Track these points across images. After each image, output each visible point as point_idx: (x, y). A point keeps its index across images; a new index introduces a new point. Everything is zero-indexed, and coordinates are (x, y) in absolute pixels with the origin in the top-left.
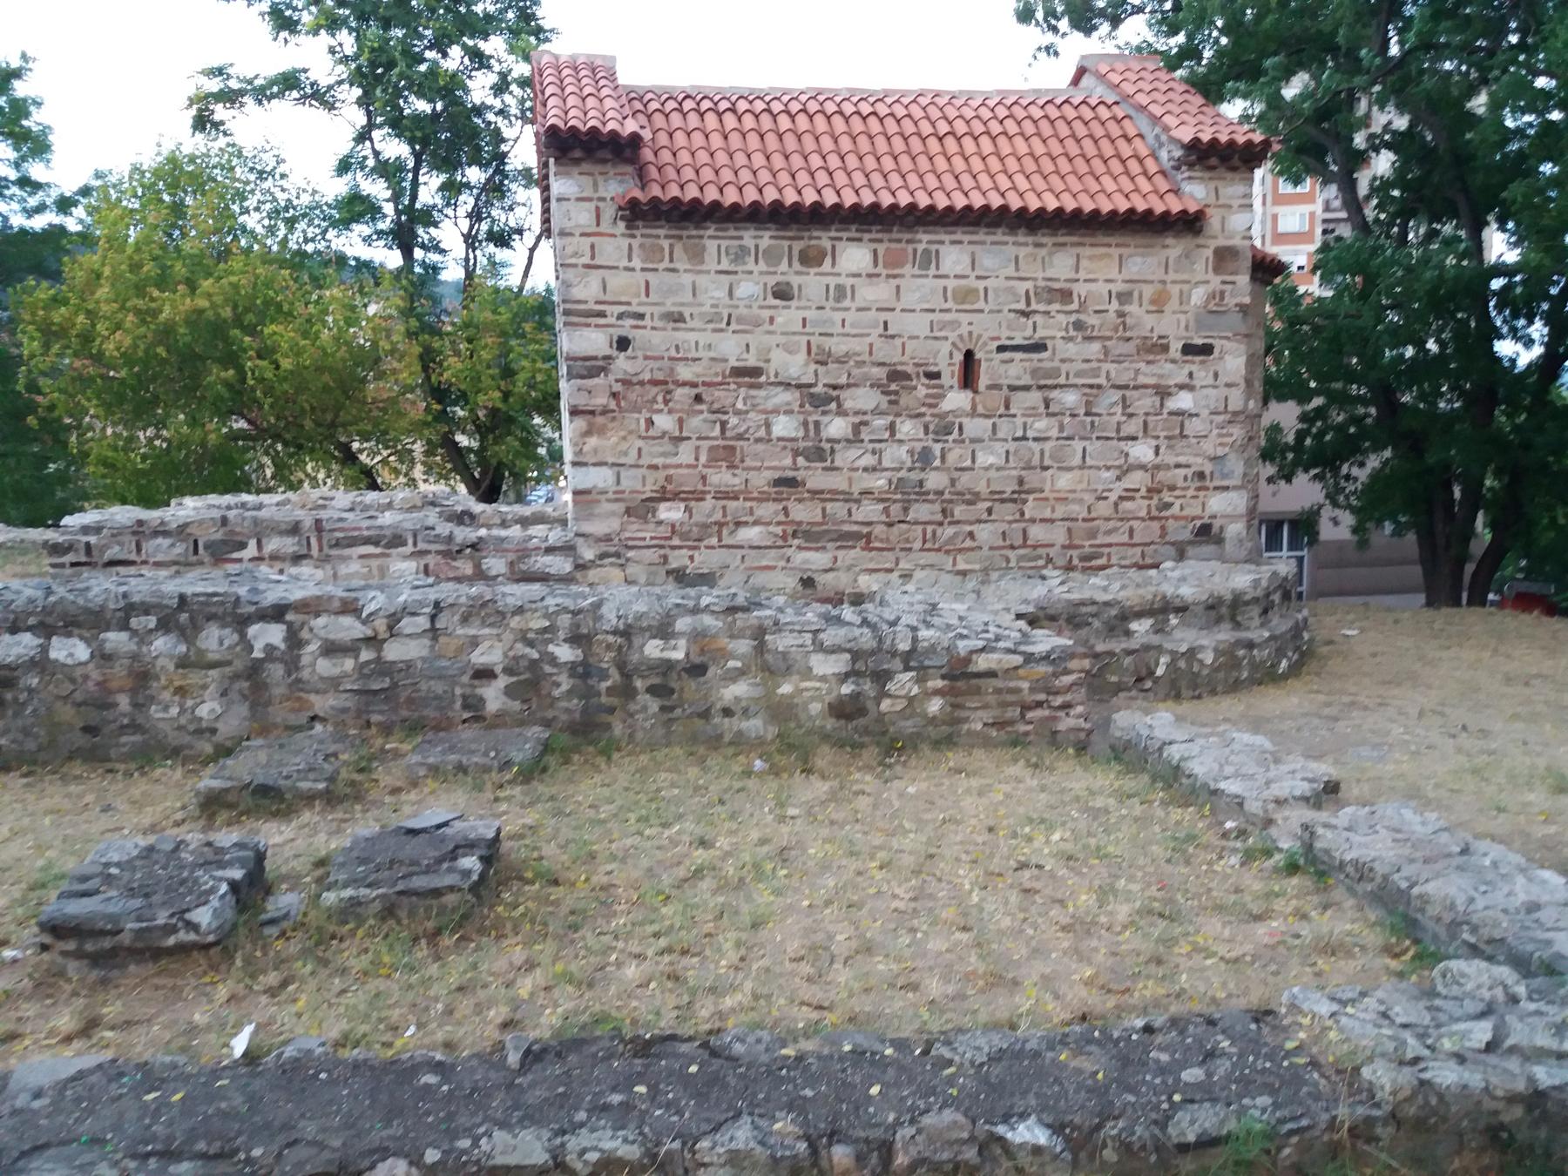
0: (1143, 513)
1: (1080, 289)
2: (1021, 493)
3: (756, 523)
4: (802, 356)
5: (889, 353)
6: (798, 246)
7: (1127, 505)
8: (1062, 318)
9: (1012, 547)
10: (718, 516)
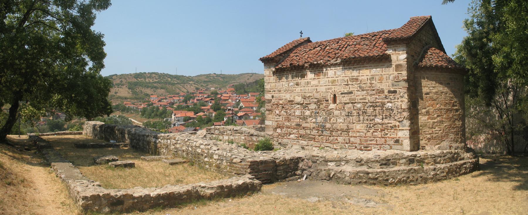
0: (380, 136)
1: (360, 78)
2: (348, 130)
3: (293, 134)
4: (301, 97)
5: (317, 96)
6: (300, 74)
7: (376, 134)
8: (356, 85)
9: (346, 143)
10: (286, 132)
